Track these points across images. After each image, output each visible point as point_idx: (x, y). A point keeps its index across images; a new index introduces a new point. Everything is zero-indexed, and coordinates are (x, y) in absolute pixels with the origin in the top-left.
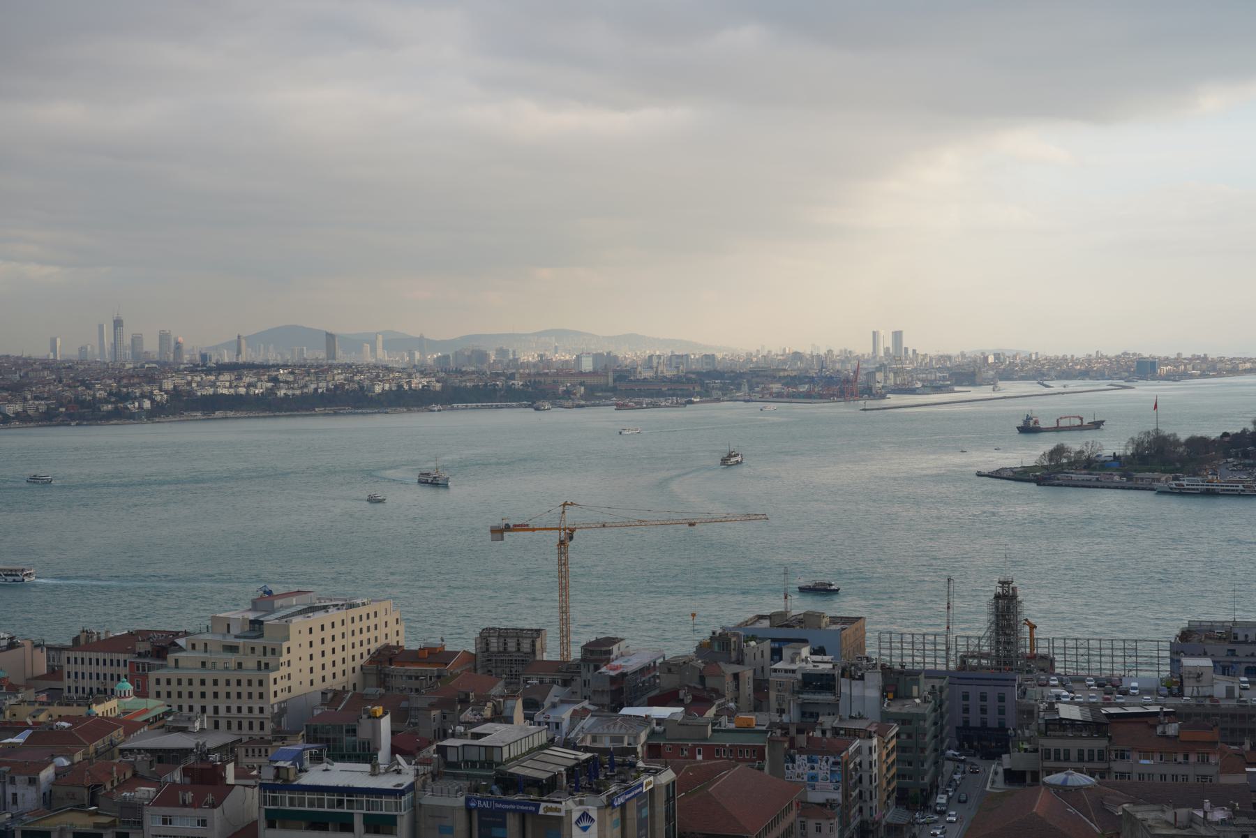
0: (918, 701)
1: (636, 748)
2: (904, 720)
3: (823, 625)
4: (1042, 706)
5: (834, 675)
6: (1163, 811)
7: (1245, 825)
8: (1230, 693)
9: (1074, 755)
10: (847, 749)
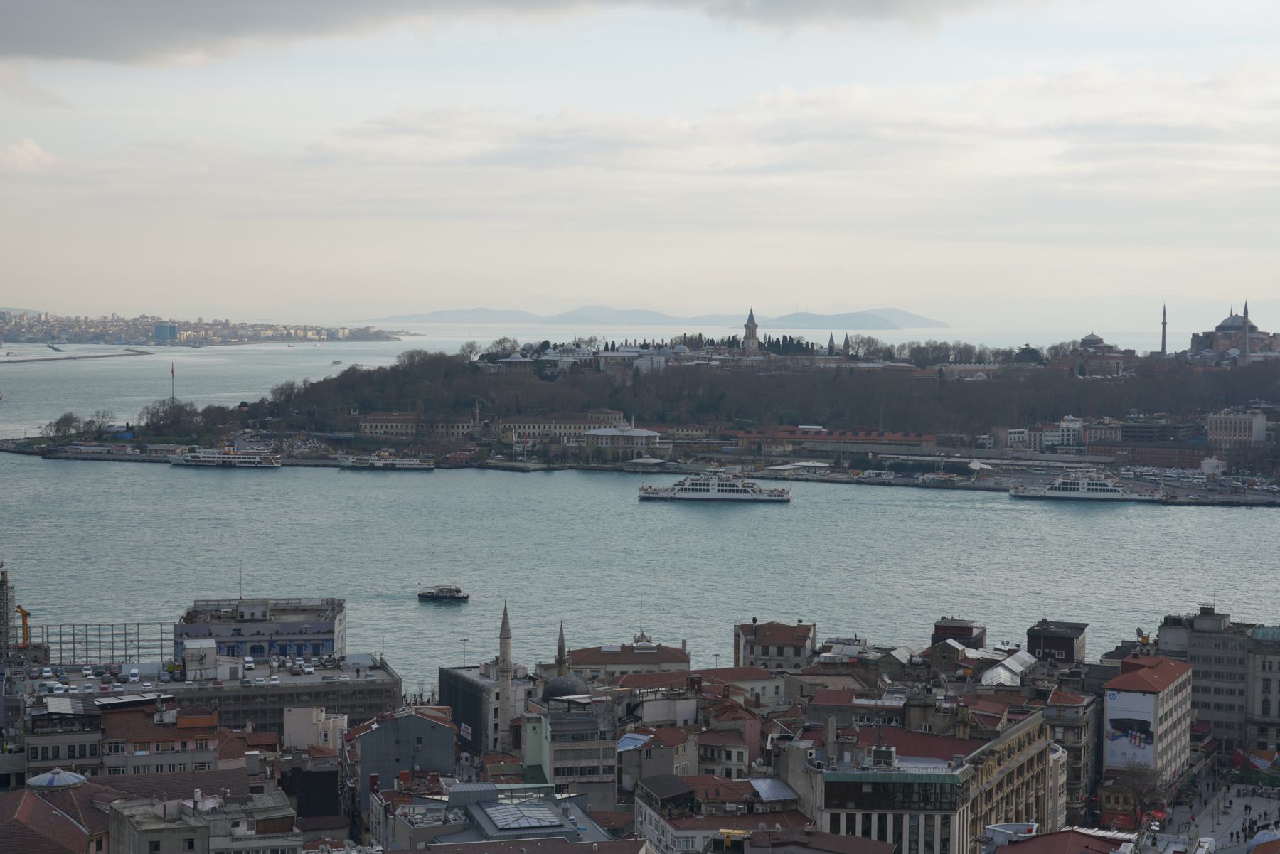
4: (30, 701)
6: (153, 805)
7: (236, 812)
8: (234, 674)
9: (63, 751)
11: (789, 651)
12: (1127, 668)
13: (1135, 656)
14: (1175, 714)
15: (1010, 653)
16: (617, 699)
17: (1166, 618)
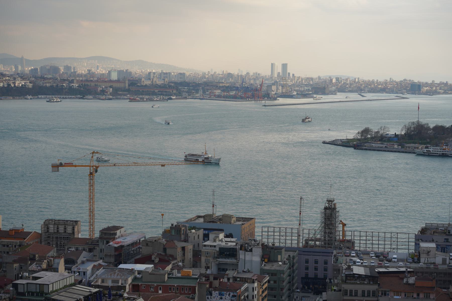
0: (280, 263)
1: (125, 287)
2: (272, 274)
3: (232, 222)
4: (345, 267)
5: (236, 249)
8: (444, 261)
9: (360, 293)
10: (240, 288)
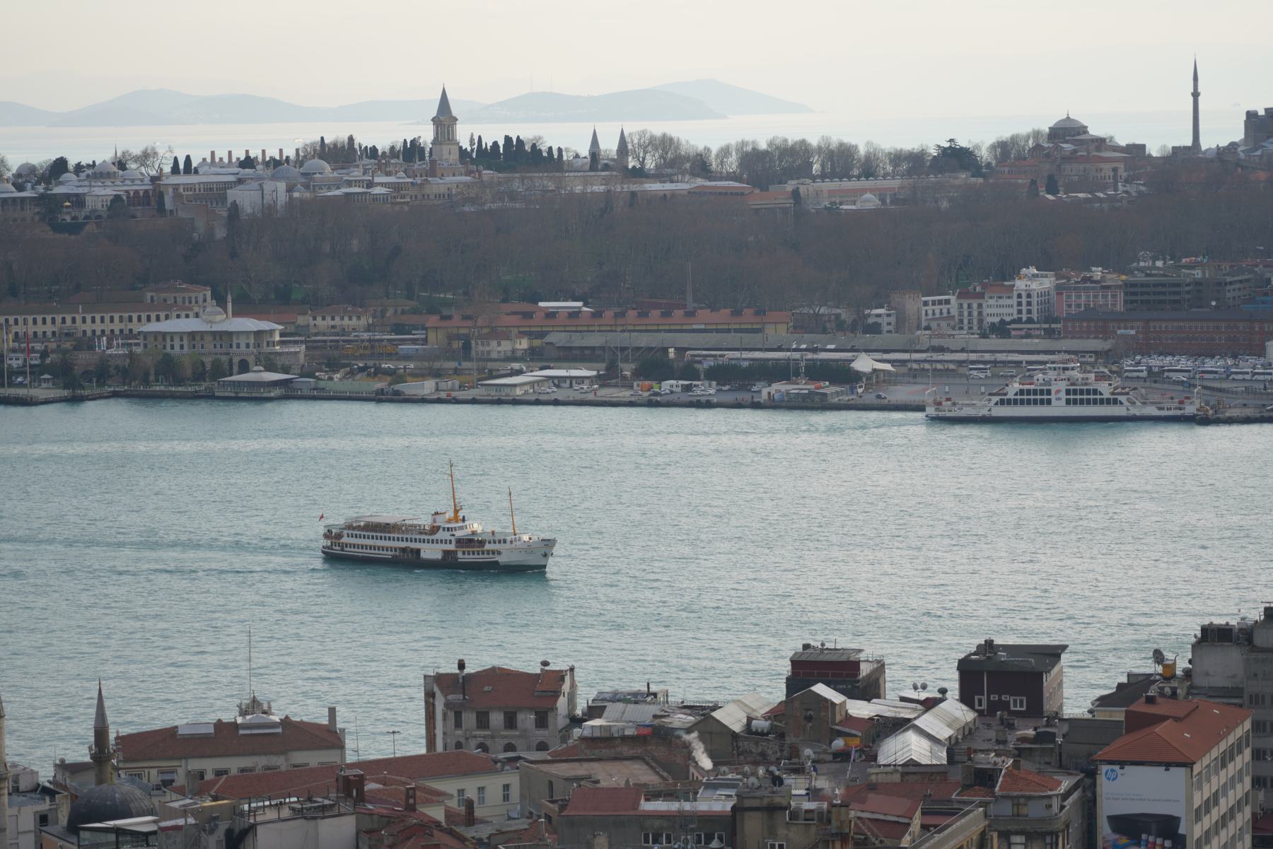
11: (527, 720)
12: (1137, 722)
13: (1150, 700)
14: (1222, 801)
15: (929, 704)
16: (208, 821)
17: (1204, 630)
